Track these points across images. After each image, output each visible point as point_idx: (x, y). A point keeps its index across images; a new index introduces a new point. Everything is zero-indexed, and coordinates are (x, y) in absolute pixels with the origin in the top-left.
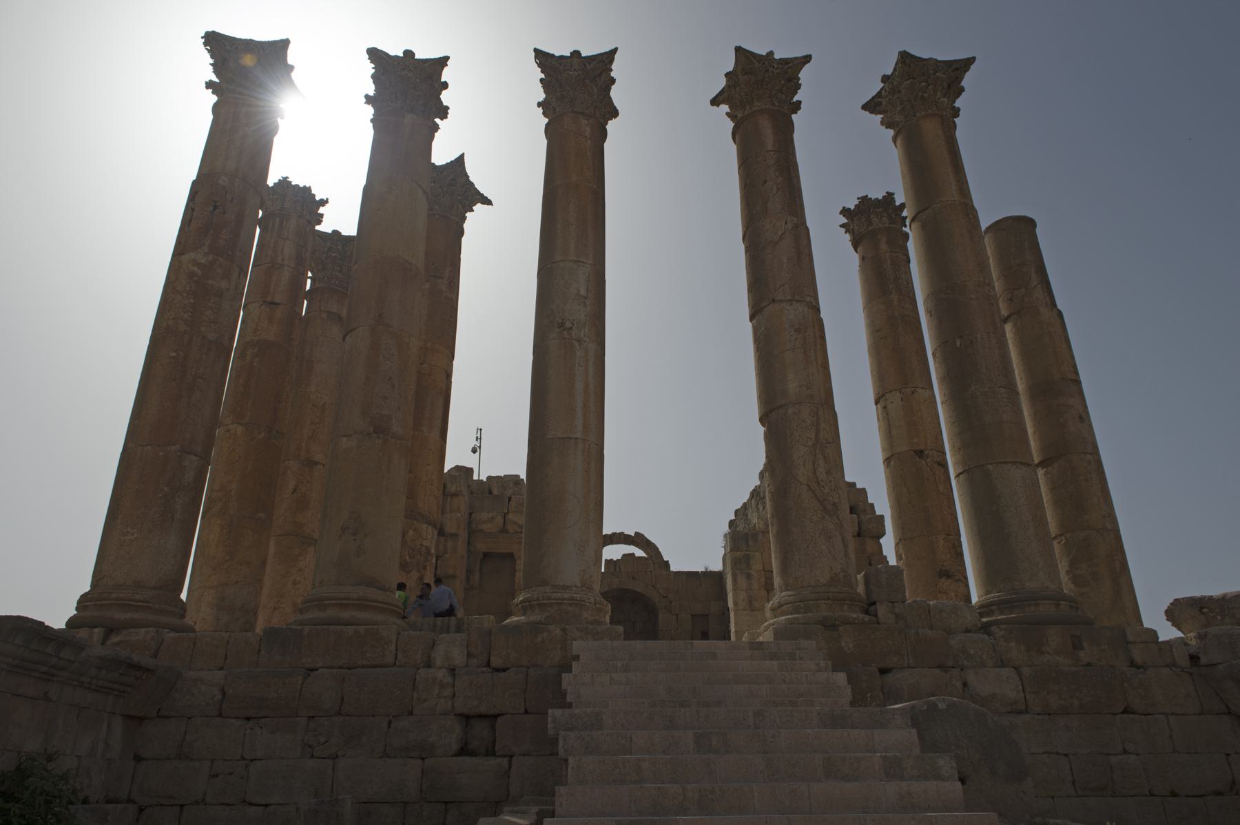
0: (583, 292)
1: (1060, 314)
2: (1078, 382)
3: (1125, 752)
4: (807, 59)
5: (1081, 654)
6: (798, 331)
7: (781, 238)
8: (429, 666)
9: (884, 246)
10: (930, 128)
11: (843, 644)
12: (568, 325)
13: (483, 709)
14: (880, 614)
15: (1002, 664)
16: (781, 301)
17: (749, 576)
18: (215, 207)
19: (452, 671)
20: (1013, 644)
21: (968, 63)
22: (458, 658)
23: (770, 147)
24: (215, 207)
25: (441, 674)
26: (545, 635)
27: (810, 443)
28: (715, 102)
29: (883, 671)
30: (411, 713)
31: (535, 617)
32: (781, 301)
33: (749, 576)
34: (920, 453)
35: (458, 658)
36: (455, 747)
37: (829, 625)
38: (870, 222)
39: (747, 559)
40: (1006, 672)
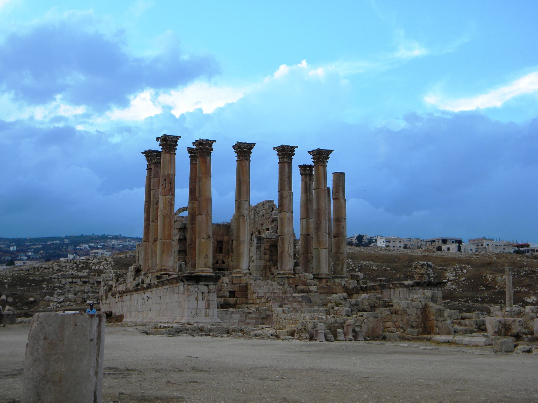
1: (345, 201)
2: (345, 218)
4: (297, 147)
8: (223, 283)
9: (308, 179)
10: (321, 168)
15: (315, 285)
17: (260, 251)
21: (332, 151)
22: (228, 282)
28: (274, 148)
29: (296, 286)
31: (239, 275)
33: (260, 251)
34: (308, 235)
35: (228, 282)
37: (288, 278)
38: (305, 169)
39: (260, 246)
40: (316, 286)
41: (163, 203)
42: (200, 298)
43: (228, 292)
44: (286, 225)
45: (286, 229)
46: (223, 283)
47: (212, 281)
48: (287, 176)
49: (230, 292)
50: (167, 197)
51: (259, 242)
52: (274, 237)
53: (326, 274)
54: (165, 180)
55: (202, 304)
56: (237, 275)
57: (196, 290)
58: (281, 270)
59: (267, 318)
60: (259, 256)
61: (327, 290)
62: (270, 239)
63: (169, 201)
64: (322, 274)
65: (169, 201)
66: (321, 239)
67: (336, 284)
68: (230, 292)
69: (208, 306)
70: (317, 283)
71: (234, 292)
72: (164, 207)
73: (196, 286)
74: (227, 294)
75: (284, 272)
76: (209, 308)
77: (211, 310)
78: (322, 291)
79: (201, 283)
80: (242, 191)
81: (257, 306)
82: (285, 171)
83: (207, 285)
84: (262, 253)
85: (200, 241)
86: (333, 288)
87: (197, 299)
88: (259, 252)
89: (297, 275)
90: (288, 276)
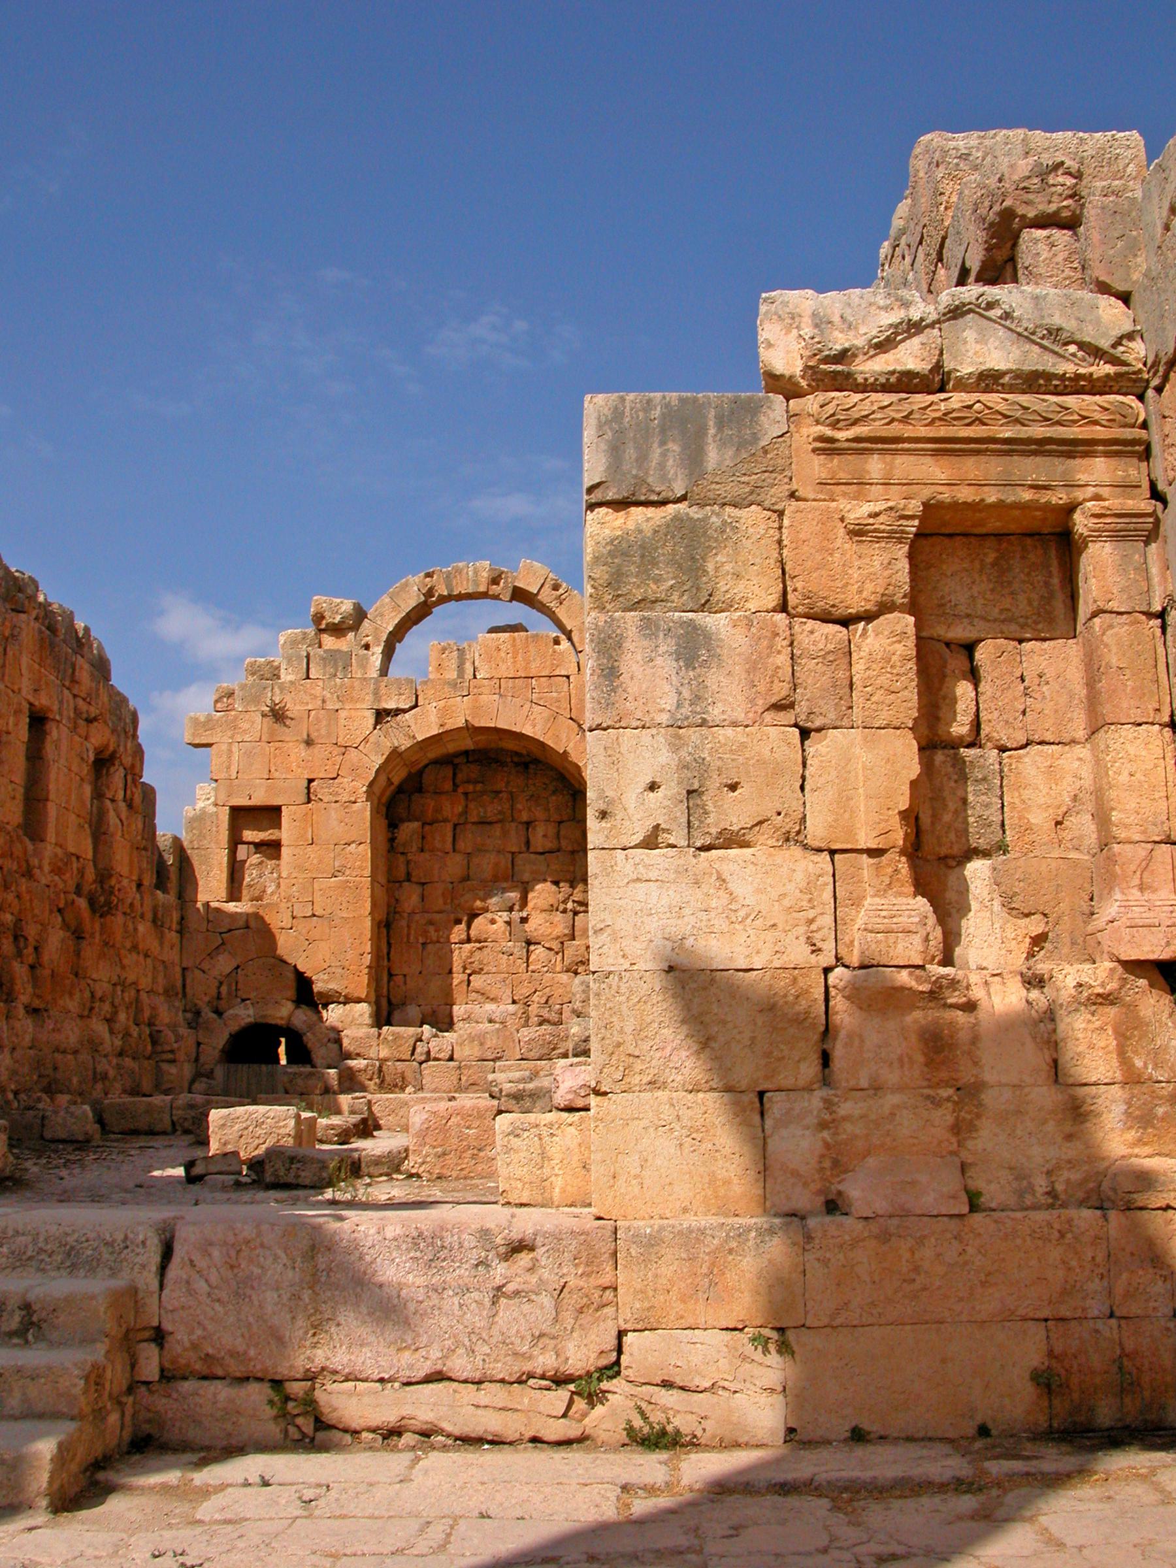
17: (693, 649)
33: (693, 649)
39: (691, 549)
62: (905, 383)
84: (729, 694)
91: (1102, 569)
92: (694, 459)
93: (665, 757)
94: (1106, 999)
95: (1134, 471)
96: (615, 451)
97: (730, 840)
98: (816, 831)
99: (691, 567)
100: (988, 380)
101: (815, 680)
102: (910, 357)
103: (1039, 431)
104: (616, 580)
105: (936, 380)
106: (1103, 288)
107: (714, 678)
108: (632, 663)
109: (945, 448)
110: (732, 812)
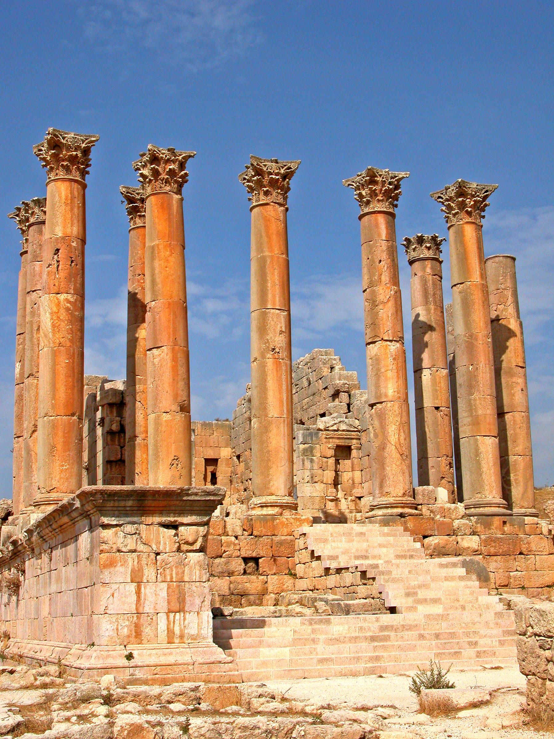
0: (284, 329)
3: (517, 570)
5: (506, 529)
6: (394, 359)
7: (388, 300)
8: (226, 534)
11: (408, 525)
12: (277, 350)
13: (254, 555)
14: (424, 510)
15: (474, 533)
16: (386, 341)
17: (312, 461)
18: (72, 262)
19: (236, 537)
20: (479, 525)
23: (384, 238)
24: (72, 262)
25: (233, 539)
26: (278, 521)
27: (397, 424)
29: (425, 537)
30: (221, 557)
32: (386, 341)
33: (312, 461)
36: (242, 571)
37: (402, 515)
39: (311, 449)
40: (476, 538)
41: (51, 314)
42: (149, 573)
43: (240, 561)
44: (389, 374)
45: (390, 385)
46: (226, 534)
47: (192, 512)
48: (384, 248)
49: (246, 560)
50: (62, 297)
51: (309, 439)
52: (343, 427)
53: (498, 505)
54: (58, 250)
55: (156, 595)
56: (265, 511)
57: (131, 543)
58: (382, 495)
59: (386, 638)
60: (307, 473)
61: (505, 548)
62: (335, 431)
63: (68, 309)
64: (489, 505)
65: (68, 309)
66: (480, 412)
67: (527, 528)
68: (246, 560)
69: (178, 604)
70: (479, 528)
71: (256, 560)
72: (53, 326)
73: (129, 528)
74: (238, 565)
75: (391, 500)
76: (181, 610)
77: (191, 618)
78: (492, 550)
79: (149, 520)
80: (269, 285)
81: (330, 597)
82: (379, 235)
83: (175, 526)
84: (316, 466)
85: (157, 419)
86: (521, 540)
87: (137, 579)
88: (308, 464)
89: (424, 510)
90: (400, 510)
91: (354, 453)
92: (312, 439)
93: (309, 473)
94: (354, 501)
95: (358, 441)
96: (304, 438)
97: (316, 482)
98: (324, 482)
99: (311, 451)
100: (343, 431)
101: (324, 465)
102: (335, 428)
103: (349, 437)
104: (304, 453)
105: (338, 430)
106: (356, 419)
107: (314, 465)
108: (306, 463)
109: (338, 438)
110: (316, 479)
